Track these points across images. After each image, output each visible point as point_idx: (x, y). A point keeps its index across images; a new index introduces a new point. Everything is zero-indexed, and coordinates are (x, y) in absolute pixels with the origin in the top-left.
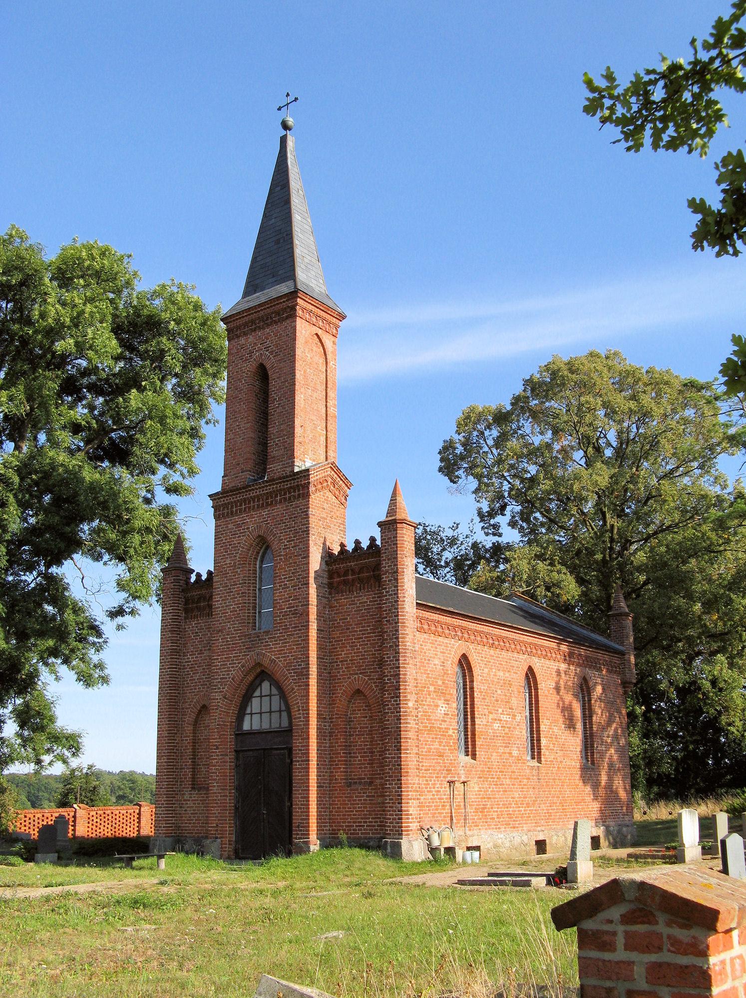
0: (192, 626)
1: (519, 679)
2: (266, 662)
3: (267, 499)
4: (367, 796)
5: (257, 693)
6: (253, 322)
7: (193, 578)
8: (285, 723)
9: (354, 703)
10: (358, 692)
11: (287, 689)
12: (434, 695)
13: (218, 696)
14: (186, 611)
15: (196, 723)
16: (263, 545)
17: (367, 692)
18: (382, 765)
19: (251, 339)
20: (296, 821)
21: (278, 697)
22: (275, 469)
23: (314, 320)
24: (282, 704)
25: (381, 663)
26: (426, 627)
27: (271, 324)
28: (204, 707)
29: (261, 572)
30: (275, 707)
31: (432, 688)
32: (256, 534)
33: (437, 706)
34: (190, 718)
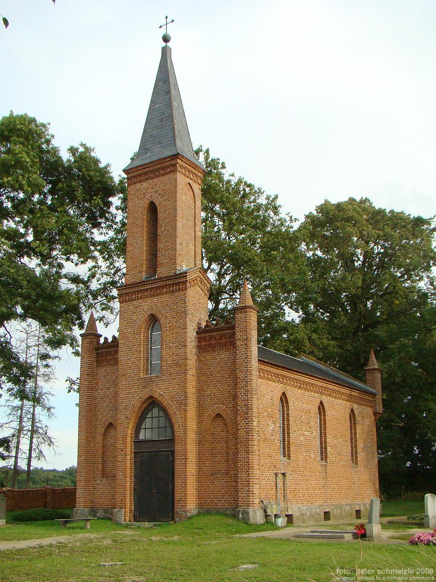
0: (102, 371)
1: (348, 411)
2: (156, 396)
3: (157, 290)
4: (224, 482)
5: (149, 415)
6: (146, 173)
7: (102, 341)
8: (169, 437)
9: (215, 423)
10: (219, 415)
11: (171, 412)
12: (266, 418)
13: (122, 417)
14: (97, 361)
15: (105, 434)
16: (153, 320)
17: (224, 415)
18: (235, 462)
19: (145, 185)
20: (177, 496)
21: (164, 418)
22: (163, 271)
23: (188, 174)
24: (167, 423)
25: (235, 397)
26: (262, 375)
27: (159, 176)
28: (111, 424)
29: (151, 338)
30: (162, 424)
31: (265, 414)
32: (149, 313)
33: (268, 425)
34: (101, 430)
